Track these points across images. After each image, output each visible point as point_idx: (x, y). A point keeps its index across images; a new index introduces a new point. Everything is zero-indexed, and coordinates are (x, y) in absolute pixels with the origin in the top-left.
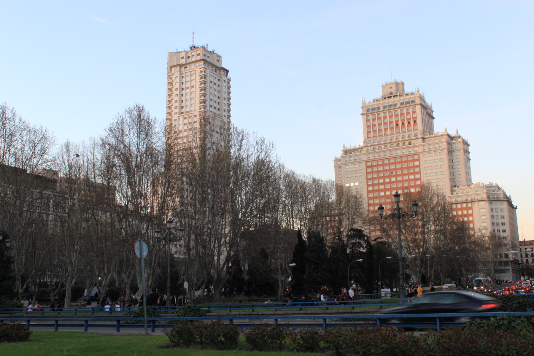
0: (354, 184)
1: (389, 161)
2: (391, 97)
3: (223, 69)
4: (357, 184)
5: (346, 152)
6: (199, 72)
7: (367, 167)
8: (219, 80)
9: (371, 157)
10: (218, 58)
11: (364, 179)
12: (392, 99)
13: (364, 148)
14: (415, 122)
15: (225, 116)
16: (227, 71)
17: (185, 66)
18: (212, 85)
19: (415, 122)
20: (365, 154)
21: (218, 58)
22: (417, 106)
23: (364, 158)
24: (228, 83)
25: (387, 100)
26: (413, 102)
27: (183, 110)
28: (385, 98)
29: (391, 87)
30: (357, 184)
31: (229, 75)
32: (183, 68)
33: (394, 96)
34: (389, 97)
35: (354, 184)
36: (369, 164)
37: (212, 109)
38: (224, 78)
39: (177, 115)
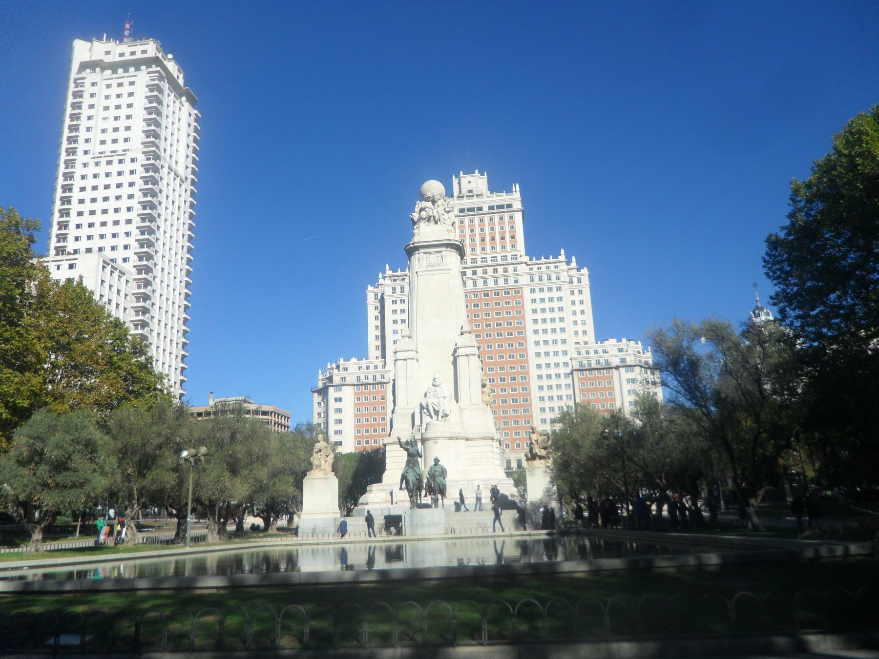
12: (475, 199)
14: (513, 237)
19: (513, 237)
22: (516, 213)
25: (465, 200)
26: (509, 206)
39: (91, 155)
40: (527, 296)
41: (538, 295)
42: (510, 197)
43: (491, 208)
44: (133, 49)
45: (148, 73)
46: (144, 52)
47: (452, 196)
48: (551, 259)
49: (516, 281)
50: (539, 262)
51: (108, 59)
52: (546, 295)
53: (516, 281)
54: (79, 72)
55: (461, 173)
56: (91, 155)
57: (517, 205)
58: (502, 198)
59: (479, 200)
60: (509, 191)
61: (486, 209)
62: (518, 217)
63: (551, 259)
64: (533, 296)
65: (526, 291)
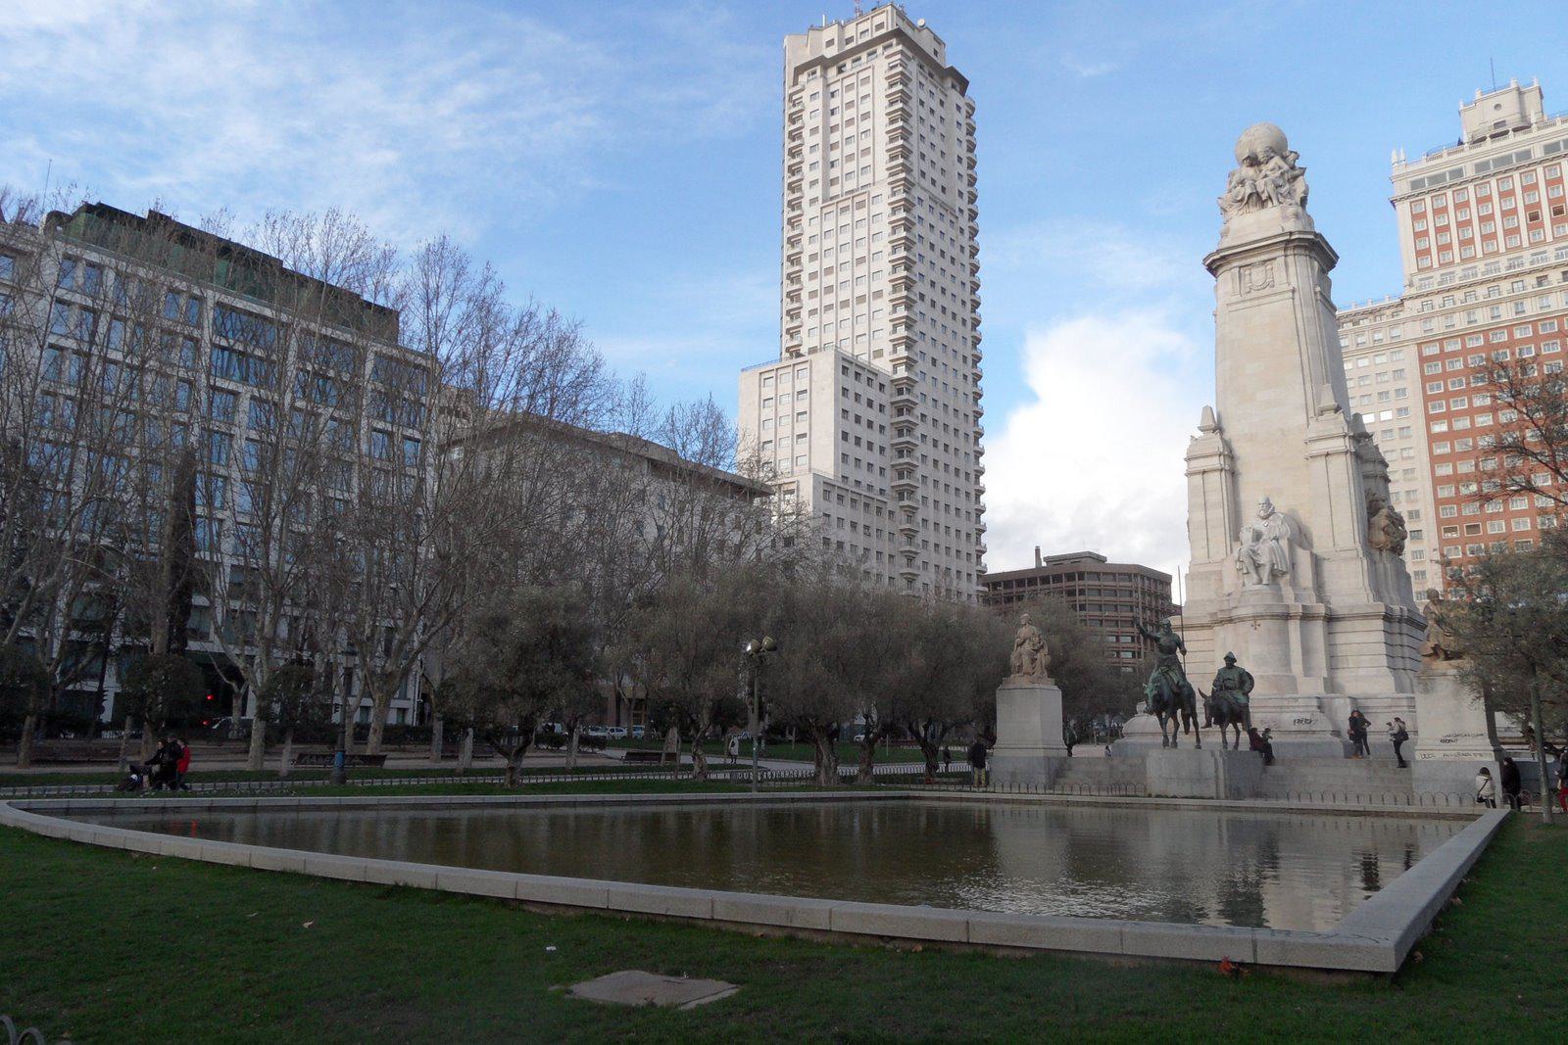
0: (1378, 416)
1: (1511, 335)
2: (1506, 132)
3: (953, 73)
4: (1386, 416)
7: (1423, 360)
9: (1438, 326)
11: (1414, 400)
12: (1512, 138)
13: (1406, 303)
15: (961, 211)
16: (962, 84)
17: (837, 62)
18: (924, 112)
20: (1413, 319)
23: (1414, 331)
25: (1488, 145)
27: (835, 190)
28: (1483, 139)
29: (1497, 106)
30: (1386, 416)
32: (832, 72)
34: (1493, 137)
35: (1378, 416)
36: (1433, 350)
38: (954, 96)
44: (862, 27)
45: (888, 57)
46: (880, 26)
51: (831, 52)
54: (795, 83)
56: (820, 204)
59: (1521, 137)
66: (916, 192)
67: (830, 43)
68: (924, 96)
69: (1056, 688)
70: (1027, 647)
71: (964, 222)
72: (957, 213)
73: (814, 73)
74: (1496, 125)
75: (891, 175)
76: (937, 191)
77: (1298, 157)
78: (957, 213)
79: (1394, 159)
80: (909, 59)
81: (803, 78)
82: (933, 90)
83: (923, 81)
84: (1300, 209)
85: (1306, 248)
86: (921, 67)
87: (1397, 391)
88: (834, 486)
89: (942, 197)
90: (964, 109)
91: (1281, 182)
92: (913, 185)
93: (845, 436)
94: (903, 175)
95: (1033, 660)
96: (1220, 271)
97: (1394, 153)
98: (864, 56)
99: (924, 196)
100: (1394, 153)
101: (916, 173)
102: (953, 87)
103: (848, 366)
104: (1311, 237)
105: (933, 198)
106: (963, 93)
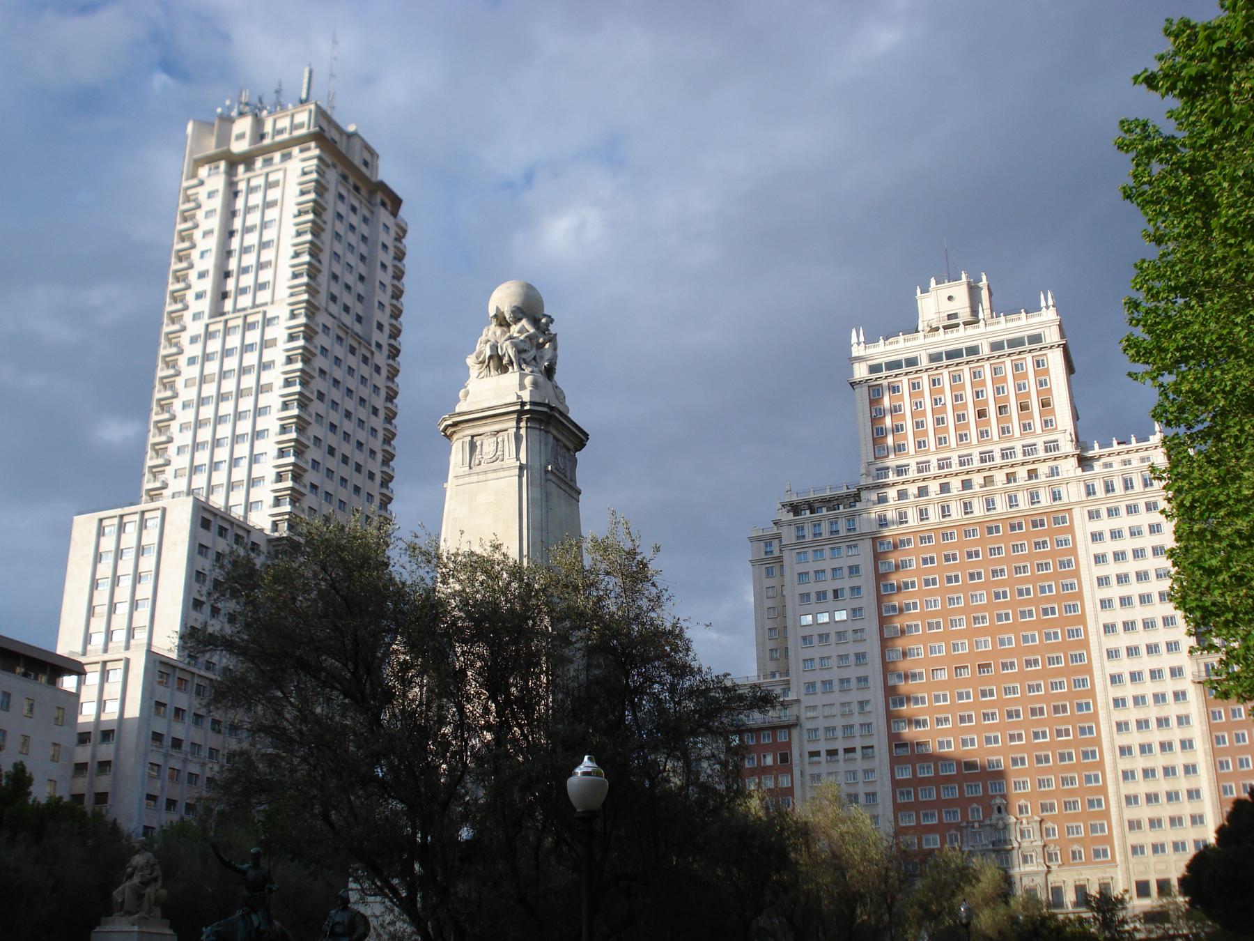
0: (832, 617)
2: (957, 325)
3: (382, 187)
4: (841, 616)
5: (795, 508)
6: (299, 172)
8: (365, 220)
10: (367, 156)
13: (864, 495)
14: (1045, 404)
15: (379, 346)
16: (394, 203)
18: (341, 228)
19: (1045, 404)
21: (367, 156)
22: (1049, 353)
24: (399, 239)
26: (1036, 339)
28: (937, 329)
29: (950, 298)
30: (841, 616)
31: (403, 212)
33: (966, 324)
34: (945, 328)
35: (832, 617)
37: (334, 309)
38: (384, 216)
40: (1082, 526)
41: (1105, 524)
42: (1035, 319)
43: (996, 346)
47: (917, 331)
48: (1134, 444)
49: (1056, 496)
50: (1106, 450)
52: (1124, 522)
53: (1056, 496)
55: (933, 281)
56: (206, 320)
57: (1052, 336)
58: (1021, 325)
59: (971, 330)
60: (1033, 308)
61: (985, 351)
62: (1055, 360)
63: (1134, 444)
64: (1095, 526)
65: (1079, 516)
66: (322, 318)
67: (240, 137)
68: (343, 209)
69: (170, 932)
70: (136, 880)
71: (381, 359)
72: (373, 348)
73: (217, 167)
74: (950, 317)
75: (292, 295)
76: (348, 320)
77: (551, 320)
78: (373, 348)
79: (854, 340)
80: (328, 166)
81: (203, 172)
82: (356, 204)
83: (344, 193)
84: (541, 379)
85: (540, 421)
86: (345, 177)
87: (852, 589)
88: (174, 667)
89: (358, 328)
90: (393, 231)
91: (527, 347)
92: (318, 309)
93: (197, 604)
94: (305, 297)
95: (140, 897)
96: (455, 437)
97: (854, 332)
98: (277, 156)
99: (330, 322)
100: (854, 332)
101: (322, 299)
102: (383, 204)
103: (207, 519)
104: (545, 409)
105: (343, 327)
106: (395, 214)
